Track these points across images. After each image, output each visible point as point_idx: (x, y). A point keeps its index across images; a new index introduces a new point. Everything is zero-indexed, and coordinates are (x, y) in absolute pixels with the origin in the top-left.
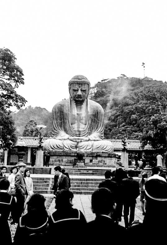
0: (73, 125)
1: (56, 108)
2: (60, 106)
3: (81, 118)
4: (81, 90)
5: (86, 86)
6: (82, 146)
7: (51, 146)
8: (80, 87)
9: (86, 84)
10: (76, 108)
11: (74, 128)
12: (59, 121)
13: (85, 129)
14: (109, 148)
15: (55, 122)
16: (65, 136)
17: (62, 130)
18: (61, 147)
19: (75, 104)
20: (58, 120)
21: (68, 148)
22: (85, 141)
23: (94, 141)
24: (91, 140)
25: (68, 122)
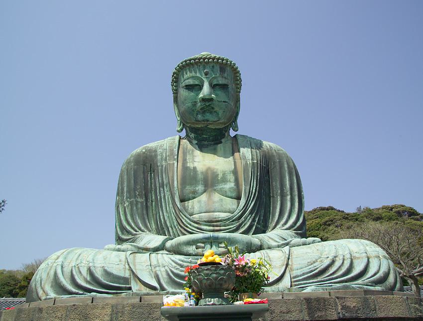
0: (189, 204)
1: (132, 158)
2: (144, 151)
4: (213, 87)
7: (56, 274)
11: (191, 215)
12: (139, 200)
13: (237, 213)
14: (384, 269)
15: (127, 204)
16: (149, 242)
17: (150, 231)
18: (117, 278)
20: (135, 196)
21: (156, 284)
24: (269, 248)
25: (168, 194)
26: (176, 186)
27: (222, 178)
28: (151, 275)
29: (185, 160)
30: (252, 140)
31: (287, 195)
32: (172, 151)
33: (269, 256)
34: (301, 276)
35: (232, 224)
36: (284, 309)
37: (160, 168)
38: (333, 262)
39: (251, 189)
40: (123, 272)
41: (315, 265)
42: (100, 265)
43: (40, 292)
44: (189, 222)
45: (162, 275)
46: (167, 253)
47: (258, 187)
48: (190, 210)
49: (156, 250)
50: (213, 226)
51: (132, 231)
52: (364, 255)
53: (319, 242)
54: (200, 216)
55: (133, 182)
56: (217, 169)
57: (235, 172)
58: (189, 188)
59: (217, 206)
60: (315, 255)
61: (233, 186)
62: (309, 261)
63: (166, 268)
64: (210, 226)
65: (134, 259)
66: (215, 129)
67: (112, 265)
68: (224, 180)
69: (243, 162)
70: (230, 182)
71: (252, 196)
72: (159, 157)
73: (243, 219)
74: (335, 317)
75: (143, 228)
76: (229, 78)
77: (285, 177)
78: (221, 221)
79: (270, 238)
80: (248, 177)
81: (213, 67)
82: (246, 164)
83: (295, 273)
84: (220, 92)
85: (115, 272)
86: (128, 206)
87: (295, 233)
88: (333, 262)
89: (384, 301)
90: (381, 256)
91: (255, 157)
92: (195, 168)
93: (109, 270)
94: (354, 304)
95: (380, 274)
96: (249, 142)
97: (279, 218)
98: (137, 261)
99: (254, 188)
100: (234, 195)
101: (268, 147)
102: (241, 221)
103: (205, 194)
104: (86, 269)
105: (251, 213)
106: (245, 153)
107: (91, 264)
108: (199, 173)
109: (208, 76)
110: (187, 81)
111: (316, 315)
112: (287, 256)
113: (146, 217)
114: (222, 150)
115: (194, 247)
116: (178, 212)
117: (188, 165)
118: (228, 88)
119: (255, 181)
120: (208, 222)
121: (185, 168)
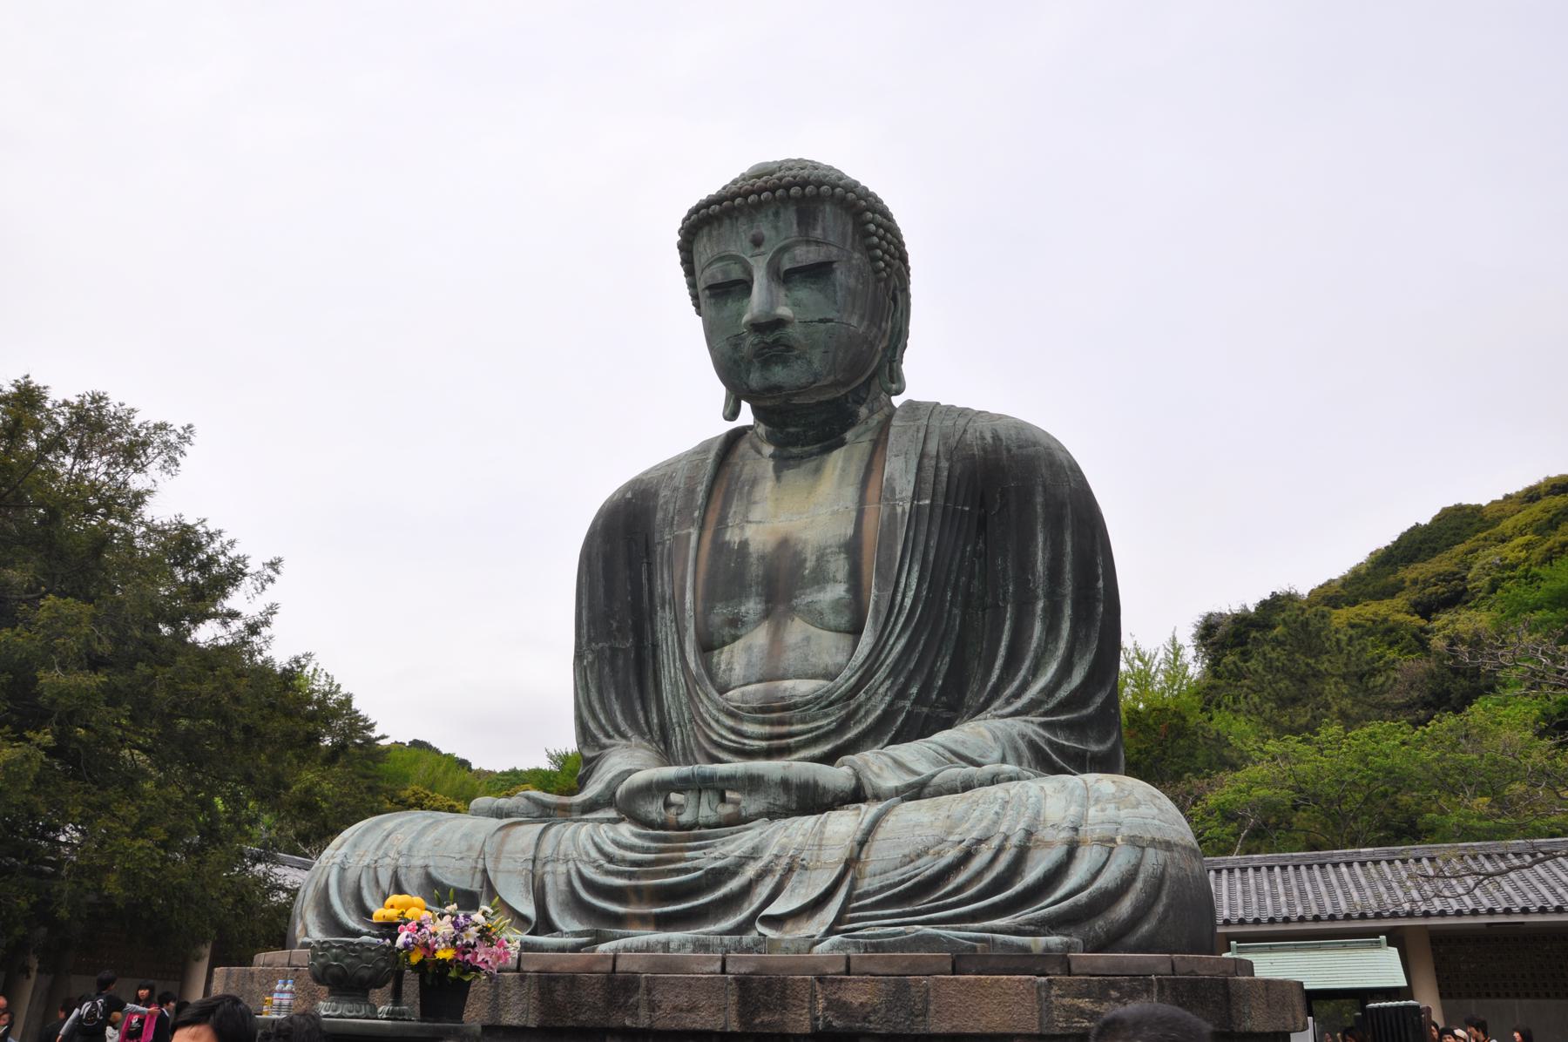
0: (722, 657)
2: (629, 495)
3: (810, 564)
4: (785, 278)
5: (830, 223)
6: (718, 876)
8: (757, 242)
9: (818, 198)
10: (767, 487)
11: (723, 690)
13: (845, 681)
14: (1106, 880)
17: (642, 735)
19: (768, 449)
21: (529, 910)
22: (787, 813)
23: (917, 791)
26: (688, 605)
27: (813, 571)
28: (526, 885)
29: (722, 523)
30: (935, 423)
31: (1037, 598)
32: (691, 491)
33: (822, 832)
34: (875, 892)
35: (827, 715)
36: (683, 1001)
37: (659, 548)
38: (967, 856)
39: (899, 598)
40: (469, 879)
41: (918, 863)
42: (420, 862)
43: (299, 927)
44: (714, 712)
45: (556, 883)
46: (612, 814)
47: (925, 586)
48: (722, 677)
49: (591, 806)
50: (772, 723)
51: (601, 736)
52: (1065, 835)
53: (1011, 779)
54: (743, 694)
55: (601, 590)
56: (805, 542)
57: (852, 548)
58: (721, 612)
59: (791, 659)
60: (926, 835)
61: (843, 593)
62: (906, 851)
63: (571, 864)
64: (763, 722)
65: (502, 843)
66: (820, 403)
67: (446, 861)
68: (820, 578)
69: (885, 510)
70: (835, 581)
71: (902, 620)
72: (660, 515)
73: (862, 696)
74: (805, 1027)
75: (624, 727)
76: (831, 239)
77: (1033, 537)
78: (795, 706)
79: (895, 761)
80: (891, 559)
81: (776, 214)
82: (893, 515)
83: (866, 885)
84: (804, 293)
85: (450, 879)
86: (592, 664)
87: (1042, 725)
88: (967, 856)
89: (960, 992)
90: (1119, 840)
91: (928, 488)
92: (744, 544)
93: (435, 873)
94: (863, 999)
95: (1083, 896)
96: (921, 435)
97: (1000, 678)
98: (509, 847)
99: (911, 594)
100: (844, 621)
101: (989, 439)
102: (853, 704)
103: (766, 624)
104: (390, 872)
105: (894, 672)
106: (897, 475)
107: (401, 861)
108: (753, 559)
109: (762, 249)
110: (708, 272)
111: (757, 1021)
112: (859, 836)
113: (635, 695)
114: (837, 472)
115: (660, 803)
116: (692, 681)
117: (728, 537)
118: (832, 271)
119: (916, 568)
120: (762, 710)
121: (719, 547)
